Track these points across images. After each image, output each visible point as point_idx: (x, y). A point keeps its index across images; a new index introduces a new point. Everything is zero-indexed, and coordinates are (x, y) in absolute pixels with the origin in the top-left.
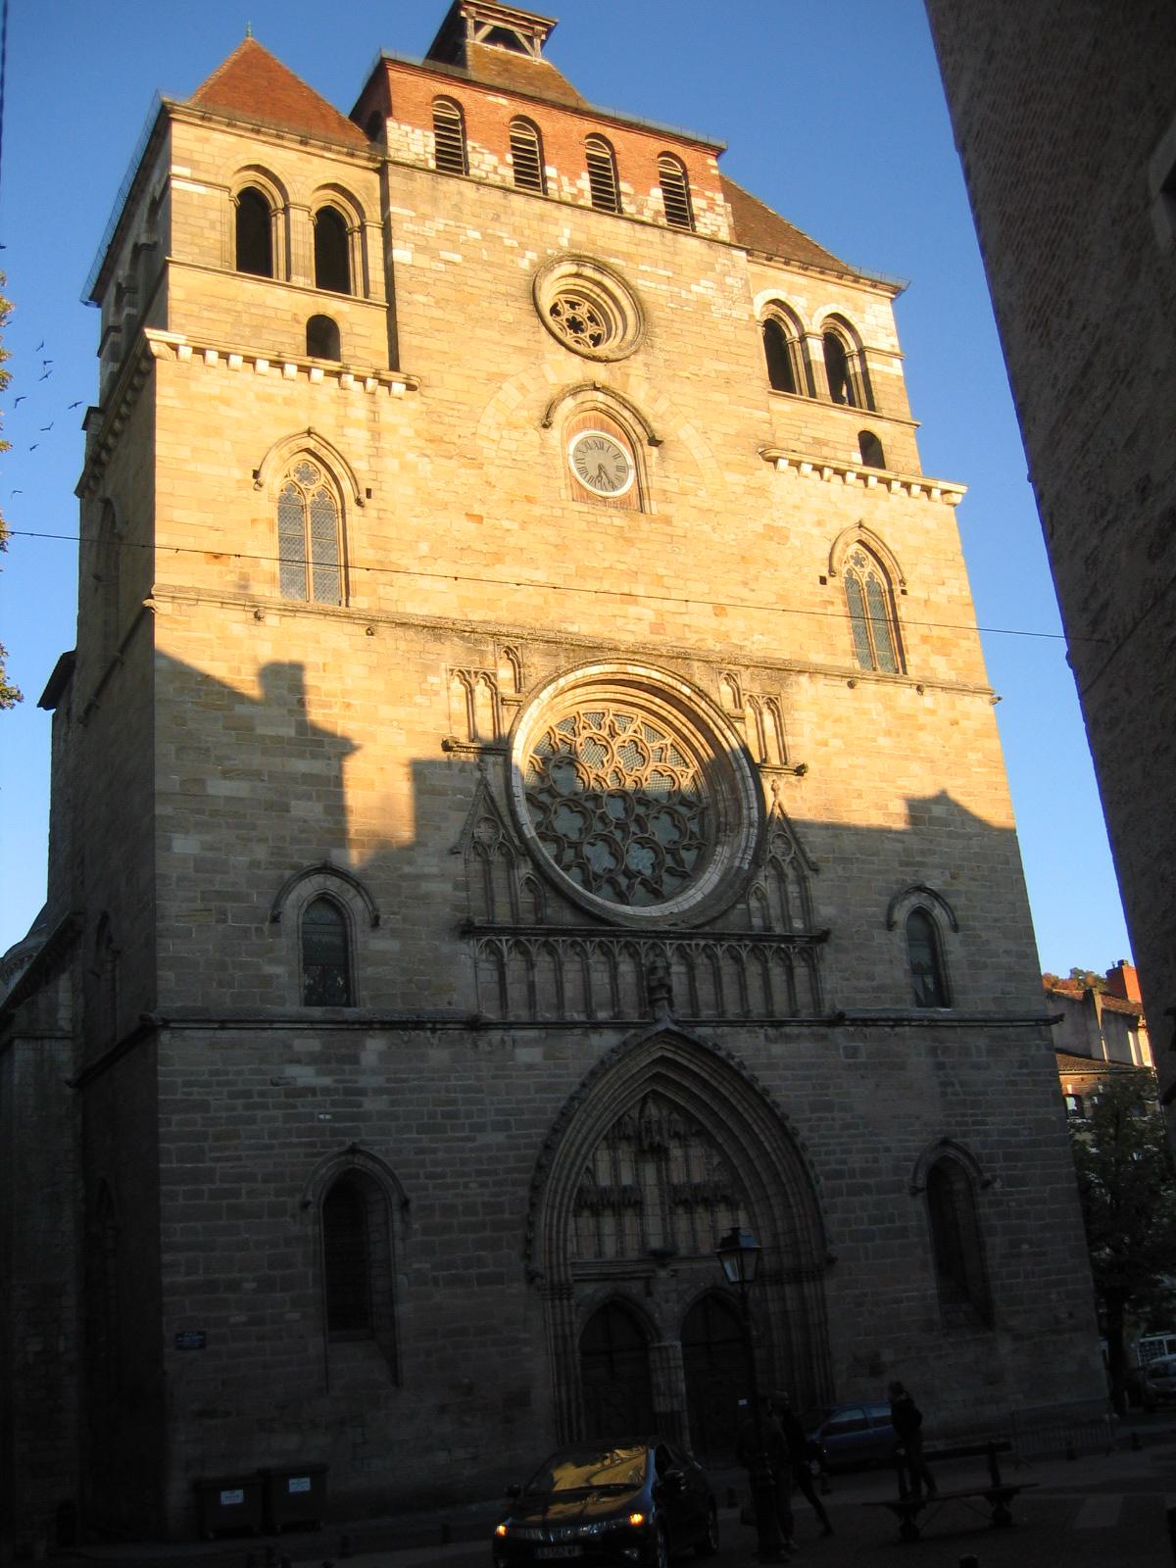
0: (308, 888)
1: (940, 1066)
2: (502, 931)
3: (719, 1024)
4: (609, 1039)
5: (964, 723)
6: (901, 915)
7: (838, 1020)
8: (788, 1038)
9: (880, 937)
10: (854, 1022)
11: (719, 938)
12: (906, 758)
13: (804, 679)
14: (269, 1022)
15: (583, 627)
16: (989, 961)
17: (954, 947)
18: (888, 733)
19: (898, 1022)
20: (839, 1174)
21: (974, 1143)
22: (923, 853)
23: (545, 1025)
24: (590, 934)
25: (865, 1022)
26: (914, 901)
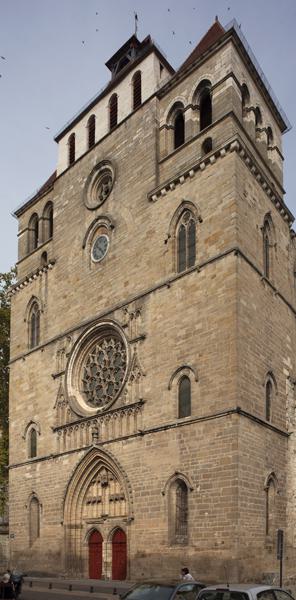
0: (29, 429)
1: (182, 442)
2: (61, 428)
3: (108, 442)
4: (83, 453)
5: (218, 275)
6: (175, 381)
7: (142, 434)
8: (129, 442)
9: (165, 393)
10: (150, 431)
11: (112, 412)
12: (188, 308)
13: (151, 295)
14: (22, 464)
15: (87, 318)
16: (210, 390)
17: (196, 389)
18: (182, 300)
19: (166, 428)
20: (139, 489)
21: (191, 472)
22: (188, 350)
23: (69, 453)
24: (79, 422)
25: (154, 431)
26: (181, 373)
